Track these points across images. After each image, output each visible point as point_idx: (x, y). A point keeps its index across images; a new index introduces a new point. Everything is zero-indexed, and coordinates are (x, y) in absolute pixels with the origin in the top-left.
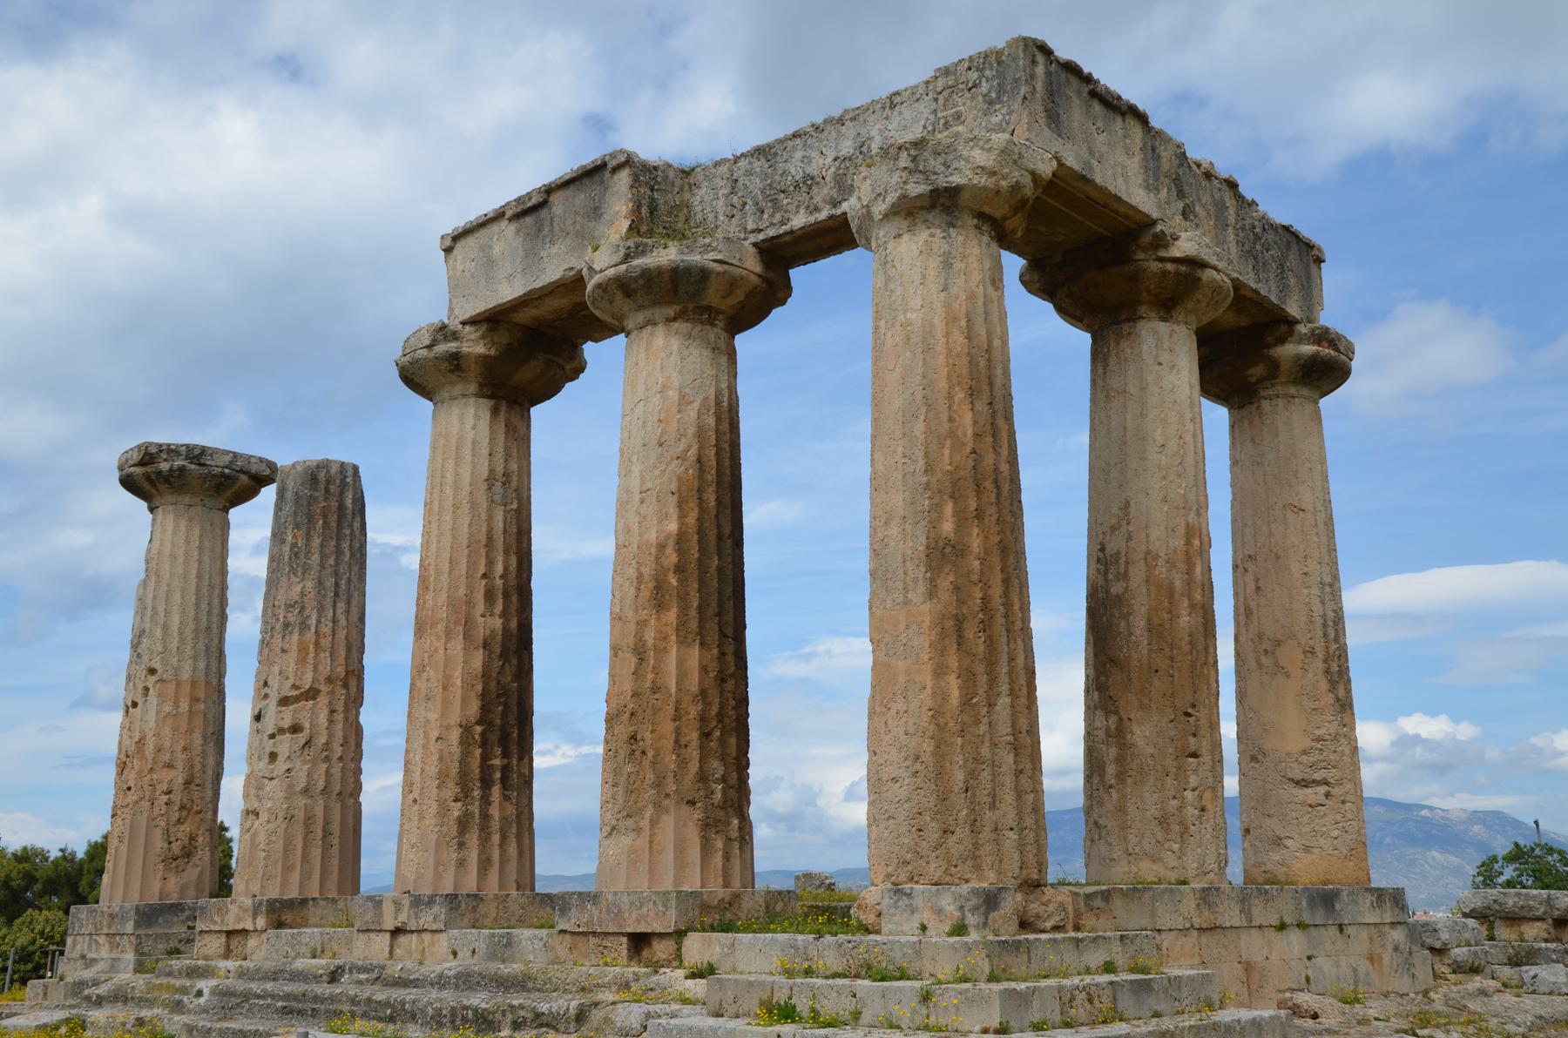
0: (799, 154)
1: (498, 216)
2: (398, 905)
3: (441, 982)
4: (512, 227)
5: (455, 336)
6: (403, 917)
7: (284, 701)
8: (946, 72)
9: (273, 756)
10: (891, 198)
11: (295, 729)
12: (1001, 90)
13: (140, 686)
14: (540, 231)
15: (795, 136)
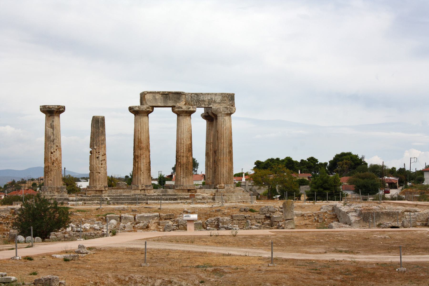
0: (202, 96)
1: (159, 93)
2: (142, 187)
3: (159, 195)
4: (160, 96)
5: (149, 108)
6: (144, 188)
7: (103, 155)
8: (224, 94)
9: (102, 164)
10: (226, 113)
11: (104, 160)
12: (232, 99)
13: (55, 149)
14: (167, 98)
15: (201, 94)
